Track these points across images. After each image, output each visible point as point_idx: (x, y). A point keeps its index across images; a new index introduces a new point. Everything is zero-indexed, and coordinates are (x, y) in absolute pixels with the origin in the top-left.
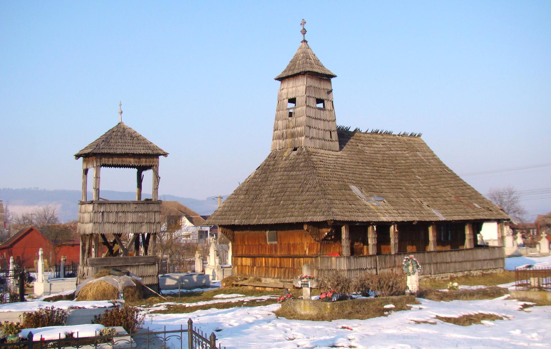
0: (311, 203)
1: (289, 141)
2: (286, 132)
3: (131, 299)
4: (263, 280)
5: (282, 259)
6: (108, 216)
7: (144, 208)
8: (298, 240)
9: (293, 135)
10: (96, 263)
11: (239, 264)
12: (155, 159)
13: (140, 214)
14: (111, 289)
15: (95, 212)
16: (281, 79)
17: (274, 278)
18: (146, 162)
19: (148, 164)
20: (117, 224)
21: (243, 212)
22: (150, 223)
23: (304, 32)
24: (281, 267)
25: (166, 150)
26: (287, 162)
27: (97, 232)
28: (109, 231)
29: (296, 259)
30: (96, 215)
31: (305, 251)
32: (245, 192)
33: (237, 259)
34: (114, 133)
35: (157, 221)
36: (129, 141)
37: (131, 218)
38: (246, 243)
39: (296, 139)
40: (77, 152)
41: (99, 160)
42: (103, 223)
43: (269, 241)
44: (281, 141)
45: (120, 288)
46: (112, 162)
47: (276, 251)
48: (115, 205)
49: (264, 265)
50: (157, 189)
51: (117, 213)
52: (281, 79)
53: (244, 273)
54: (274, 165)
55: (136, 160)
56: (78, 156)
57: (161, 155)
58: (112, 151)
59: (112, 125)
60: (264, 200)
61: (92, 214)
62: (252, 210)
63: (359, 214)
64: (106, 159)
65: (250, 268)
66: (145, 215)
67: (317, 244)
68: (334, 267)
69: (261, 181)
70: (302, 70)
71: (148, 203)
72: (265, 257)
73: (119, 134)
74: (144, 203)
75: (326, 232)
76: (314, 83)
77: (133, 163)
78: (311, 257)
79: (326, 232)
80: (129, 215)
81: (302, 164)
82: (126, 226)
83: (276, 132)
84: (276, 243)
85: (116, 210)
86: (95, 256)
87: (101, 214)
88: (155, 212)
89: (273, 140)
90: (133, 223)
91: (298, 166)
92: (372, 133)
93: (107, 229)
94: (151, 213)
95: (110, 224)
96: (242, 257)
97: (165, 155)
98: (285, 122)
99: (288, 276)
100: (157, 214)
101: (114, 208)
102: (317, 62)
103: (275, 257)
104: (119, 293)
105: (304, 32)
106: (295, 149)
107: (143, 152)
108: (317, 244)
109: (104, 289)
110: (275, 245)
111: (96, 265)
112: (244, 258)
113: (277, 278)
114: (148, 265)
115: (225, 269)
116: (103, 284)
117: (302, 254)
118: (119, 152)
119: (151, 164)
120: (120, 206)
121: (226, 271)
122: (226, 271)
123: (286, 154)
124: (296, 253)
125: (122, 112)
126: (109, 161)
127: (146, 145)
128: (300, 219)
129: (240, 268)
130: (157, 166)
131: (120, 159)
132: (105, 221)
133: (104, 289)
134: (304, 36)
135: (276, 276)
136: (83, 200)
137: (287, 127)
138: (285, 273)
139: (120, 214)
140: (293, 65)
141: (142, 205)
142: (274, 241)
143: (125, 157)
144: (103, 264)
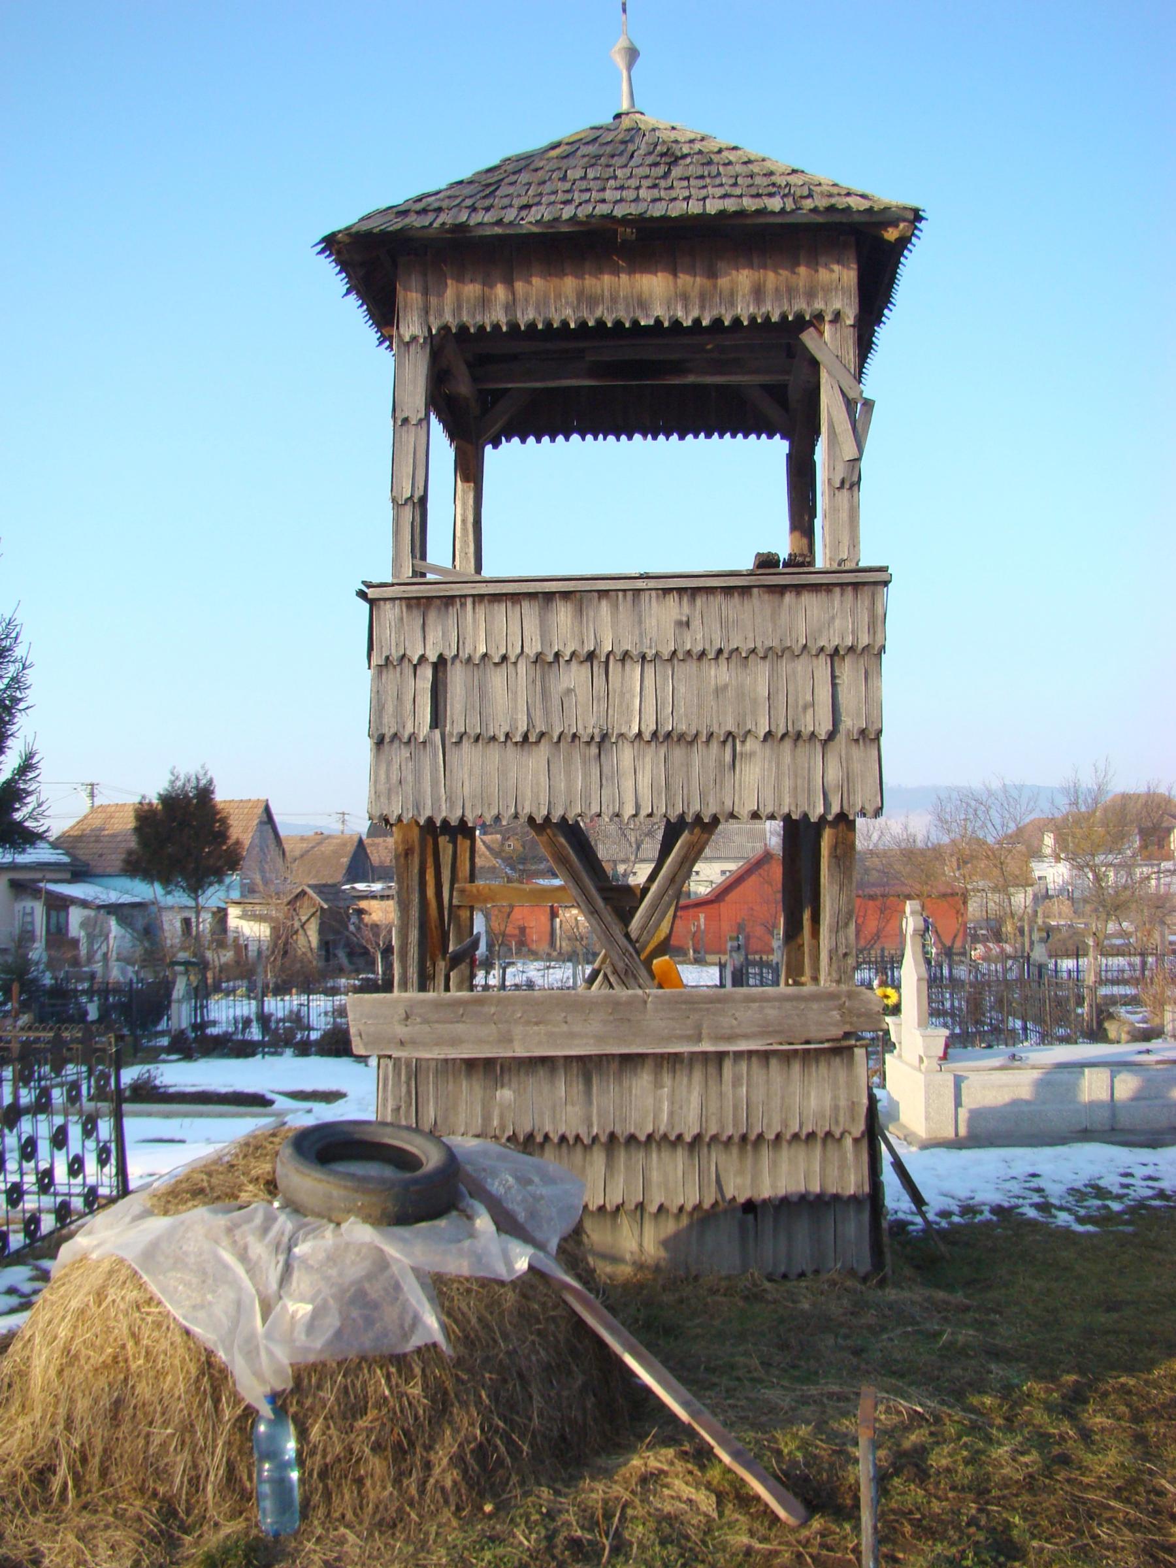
7: (751, 622)
18: (758, 293)
20: (544, 749)
30: (390, 676)
37: (639, 700)
48: (530, 610)
55: (684, 279)
64: (472, 290)
66: (759, 678)
71: (779, 590)
74: (745, 591)
77: (659, 311)
85: (532, 649)
87: (427, 672)
94: (801, 666)
95: (494, 751)
101: (516, 631)
119: (800, 305)
120: (563, 614)
126: (484, 303)
131: (569, 284)
139: (575, 677)
143: (599, 271)
144: (455, 1042)
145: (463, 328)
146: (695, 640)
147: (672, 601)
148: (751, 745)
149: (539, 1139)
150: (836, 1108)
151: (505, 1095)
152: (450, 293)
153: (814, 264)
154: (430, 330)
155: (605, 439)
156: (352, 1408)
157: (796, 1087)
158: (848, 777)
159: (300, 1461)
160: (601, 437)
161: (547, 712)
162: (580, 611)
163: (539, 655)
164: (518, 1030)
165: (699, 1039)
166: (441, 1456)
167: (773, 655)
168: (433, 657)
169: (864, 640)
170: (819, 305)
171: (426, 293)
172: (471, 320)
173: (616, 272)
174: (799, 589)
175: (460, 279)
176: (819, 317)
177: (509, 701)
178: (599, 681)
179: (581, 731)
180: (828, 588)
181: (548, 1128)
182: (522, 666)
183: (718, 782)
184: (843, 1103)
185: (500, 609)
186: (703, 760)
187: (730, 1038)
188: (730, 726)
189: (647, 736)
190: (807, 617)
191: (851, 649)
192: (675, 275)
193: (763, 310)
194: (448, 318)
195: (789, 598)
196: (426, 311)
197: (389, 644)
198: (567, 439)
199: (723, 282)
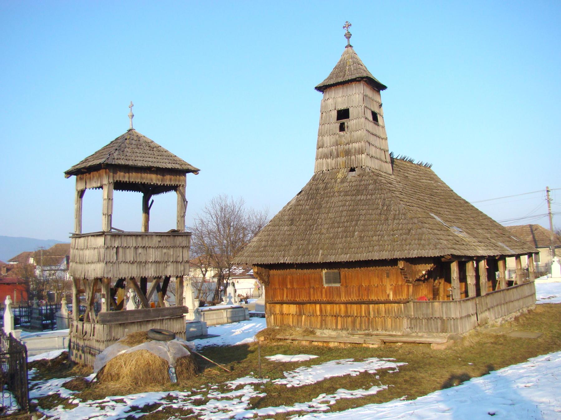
0: (408, 234)
1: (341, 160)
2: (337, 150)
3: (185, 375)
4: (318, 332)
5: (349, 306)
6: (125, 253)
7: (169, 241)
8: (375, 281)
9: (348, 153)
10: (108, 319)
11: (278, 312)
12: (182, 178)
13: (165, 251)
14: (158, 363)
15: (108, 248)
16: (322, 89)
17: (336, 329)
18: (171, 180)
19: (173, 183)
20: (136, 264)
21: (295, 247)
23: (348, 36)
24: (347, 316)
25: (195, 165)
26: (345, 184)
27: (110, 276)
28: (125, 274)
29: (371, 306)
30: (108, 251)
31: (388, 296)
32: (290, 223)
33: (274, 307)
34: (127, 141)
35: (185, 259)
36: (148, 151)
37: (153, 255)
38: (289, 286)
39: (353, 157)
40: (69, 168)
41: (111, 174)
42: (117, 262)
43: (326, 283)
44: (329, 160)
45: (171, 359)
46: (129, 178)
47: (339, 295)
48: (134, 238)
49: (318, 313)
50: (184, 216)
51: (136, 248)
52: (322, 89)
53: (285, 323)
54: (325, 188)
55: (159, 176)
56: (69, 174)
57: (189, 171)
58: (130, 163)
59: (123, 131)
60: (324, 231)
61: (102, 251)
62: (308, 244)
63: (381, 248)
64: (122, 174)
65: (295, 317)
66: (171, 252)
67: (408, 286)
68: (437, 315)
69: (310, 209)
70: (358, 76)
71: (175, 236)
72: (320, 303)
73: (134, 142)
74: (169, 236)
75: (423, 269)
76: (369, 92)
77: (154, 182)
78: (399, 303)
79: (423, 269)
80: (151, 251)
81: (371, 187)
82: (147, 266)
83: (320, 150)
84: (338, 285)
85: (134, 245)
86: (107, 310)
87: (115, 249)
88: (183, 247)
89: (317, 159)
90: (156, 262)
91: (366, 189)
92: (400, 159)
93: (123, 271)
94: (178, 249)
95: (127, 265)
96: (282, 303)
97: (196, 171)
98: (333, 139)
99: (361, 326)
100: (185, 251)
101: (132, 242)
102: (366, 71)
103: (336, 304)
104: (169, 367)
105: (348, 36)
106: (352, 170)
107: (169, 166)
108: (408, 286)
109: (148, 364)
110: (337, 288)
111: (109, 321)
112: (285, 305)
113: (342, 329)
114: (173, 319)
115: (206, 312)
116: (147, 355)
117: (382, 299)
118: (140, 164)
119: (177, 183)
120: (139, 238)
121: (207, 314)
122: (207, 314)
123: (340, 175)
124: (373, 298)
125: (133, 116)
126: (124, 177)
127: (171, 158)
128: (397, 255)
129: (279, 317)
130: (184, 186)
131: (139, 175)
132: (120, 259)
133: (148, 364)
134: (349, 40)
135: (339, 327)
136: (77, 233)
137: (337, 144)
138: (354, 322)
139: (140, 251)
140: (341, 71)
141: (167, 238)
142: (335, 282)
143: (144, 173)
144: (118, 320)
145: (120, 181)
147: (158, 237)
148: (169, 263)
151: (127, 330)
152: (118, 174)
153: (180, 176)
156: (181, 364)
157: (175, 324)
158: (184, 269)
159: (175, 373)
161: (136, 257)
162: (142, 239)
165: (159, 317)
166: (191, 369)
167: (173, 247)
171: (114, 173)
172: (122, 179)
173: (147, 173)
174: (178, 236)
175: (120, 171)
176: (180, 185)
177: (130, 255)
178: (145, 251)
180: (182, 236)
182: (132, 248)
183: (164, 270)
185: (129, 238)
186: (162, 266)
188: (166, 260)
190: (180, 241)
194: (118, 179)
195: (176, 237)
196: (113, 177)
199: (165, 177)
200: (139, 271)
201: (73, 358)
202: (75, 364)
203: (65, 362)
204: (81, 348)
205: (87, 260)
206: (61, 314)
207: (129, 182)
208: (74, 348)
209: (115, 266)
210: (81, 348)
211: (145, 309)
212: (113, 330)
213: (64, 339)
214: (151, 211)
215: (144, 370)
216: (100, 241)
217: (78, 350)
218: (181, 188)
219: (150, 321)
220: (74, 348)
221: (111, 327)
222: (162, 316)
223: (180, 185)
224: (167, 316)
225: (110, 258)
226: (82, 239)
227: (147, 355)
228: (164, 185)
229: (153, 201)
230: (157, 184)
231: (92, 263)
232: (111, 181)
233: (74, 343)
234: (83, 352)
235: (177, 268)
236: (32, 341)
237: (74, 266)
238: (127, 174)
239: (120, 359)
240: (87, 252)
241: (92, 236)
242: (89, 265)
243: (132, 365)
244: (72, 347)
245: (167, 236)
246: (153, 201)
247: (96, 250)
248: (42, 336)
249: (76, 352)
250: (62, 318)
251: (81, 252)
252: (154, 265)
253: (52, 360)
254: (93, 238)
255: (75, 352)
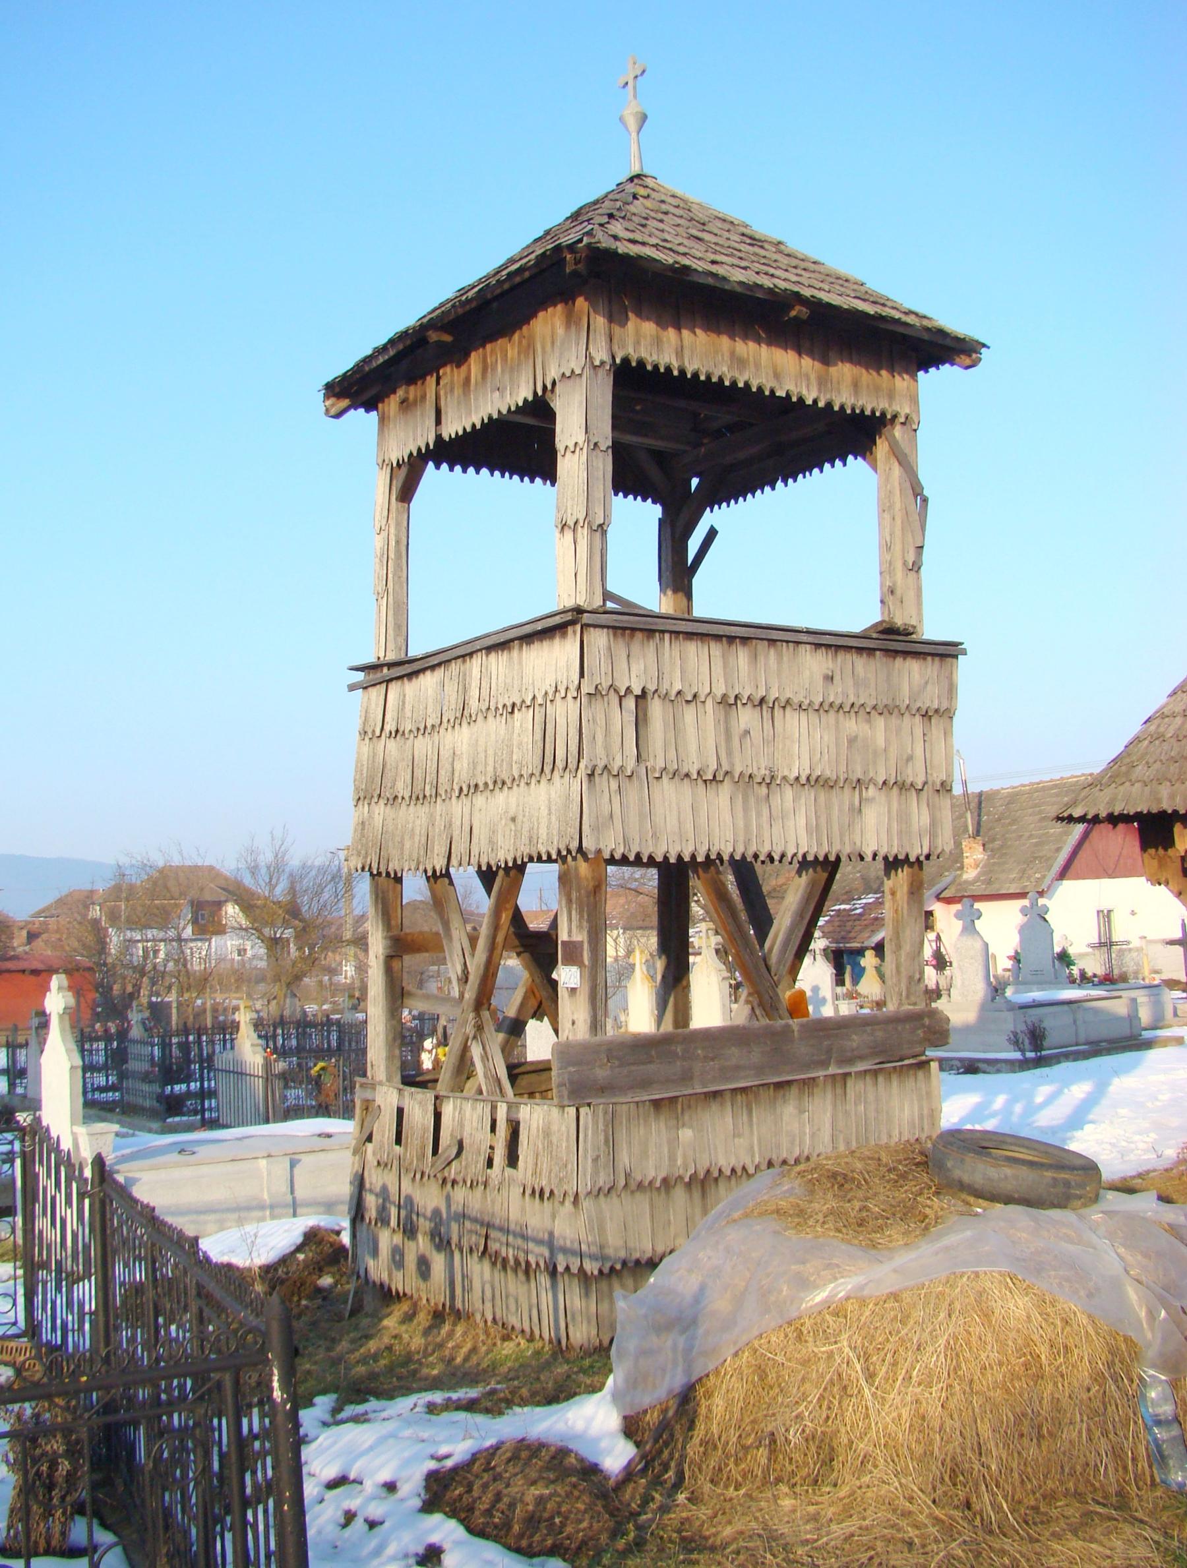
10: (601, 1073)
12: (901, 382)
13: (851, 725)
20: (726, 789)
22: (903, 787)
37: (802, 745)
41: (600, 321)
42: (642, 772)
46: (680, 353)
48: (716, 649)
51: (728, 703)
64: (649, 327)
66: (878, 731)
71: (893, 653)
74: (870, 651)
80: (792, 723)
82: (776, 800)
85: (719, 690)
87: (630, 703)
88: (926, 716)
90: (814, 782)
93: (672, 822)
109: (1034, 1371)
111: (604, 1089)
114: (889, 1074)
120: (742, 656)
131: (725, 341)
132: (658, 757)
133: (1034, 1371)
139: (746, 717)
141: (860, 663)
143: (745, 337)
144: (645, 1084)
145: (641, 363)
146: (835, 694)
147: (821, 654)
148: (872, 792)
149: (716, 1174)
150: (921, 1117)
151: (686, 1134)
152: (631, 325)
154: (614, 358)
155: (511, 478)
158: (934, 823)
160: (507, 475)
161: (730, 753)
163: (724, 696)
164: (698, 1067)
165: (824, 1064)
167: (888, 710)
168: (637, 691)
169: (945, 705)
170: (896, 408)
171: (611, 319)
173: (758, 341)
174: (906, 654)
175: (639, 315)
177: (699, 738)
178: (768, 725)
179: (755, 772)
181: (722, 1162)
182: (709, 703)
184: (925, 1112)
185: (692, 647)
187: (850, 1061)
188: (859, 774)
189: (803, 780)
191: (937, 711)
192: (800, 355)
193: (860, 403)
194: (631, 351)
195: (899, 661)
197: (599, 675)
198: (478, 472)
200: (741, 823)
201: (378, 1269)
202: (388, 1296)
203: (326, 1281)
204: (424, 1225)
205: (462, 768)
206: (238, 1062)
207: (682, 372)
208: (383, 1219)
209: (633, 793)
210: (424, 1225)
211: (764, 1021)
212: (622, 1135)
213: (293, 1164)
214: (696, 581)
215: (1008, 1415)
216: (554, 661)
217: (410, 1231)
218: (898, 432)
219: (789, 1083)
220: (383, 1219)
221: (612, 1121)
222: (842, 1062)
223: (895, 417)
224: (861, 1058)
225: (607, 747)
226: (428, 681)
227: (1016, 1307)
228: (829, 405)
229: (712, 534)
230: (801, 400)
231: (500, 784)
232: (600, 354)
233: (384, 1192)
234: (442, 1242)
235: (904, 817)
236: (163, 1174)
237: (378, 820)
238: (671, 333)
239: (830, 1337)
240: (461, 739)
241: (490, 649)
242: (480, 800)
243: (927, 1382)
244: (371, 1212)
245: (860, 650)
246: (712, 534)
247: (523, 719)
248: (203, 1151)
249: (398, 1239)
250: (240, 1074)
251: (422, 746)
252: (808, 795)
253: (267, 1269)
254: (498, 663)
255: (386, 1239)
